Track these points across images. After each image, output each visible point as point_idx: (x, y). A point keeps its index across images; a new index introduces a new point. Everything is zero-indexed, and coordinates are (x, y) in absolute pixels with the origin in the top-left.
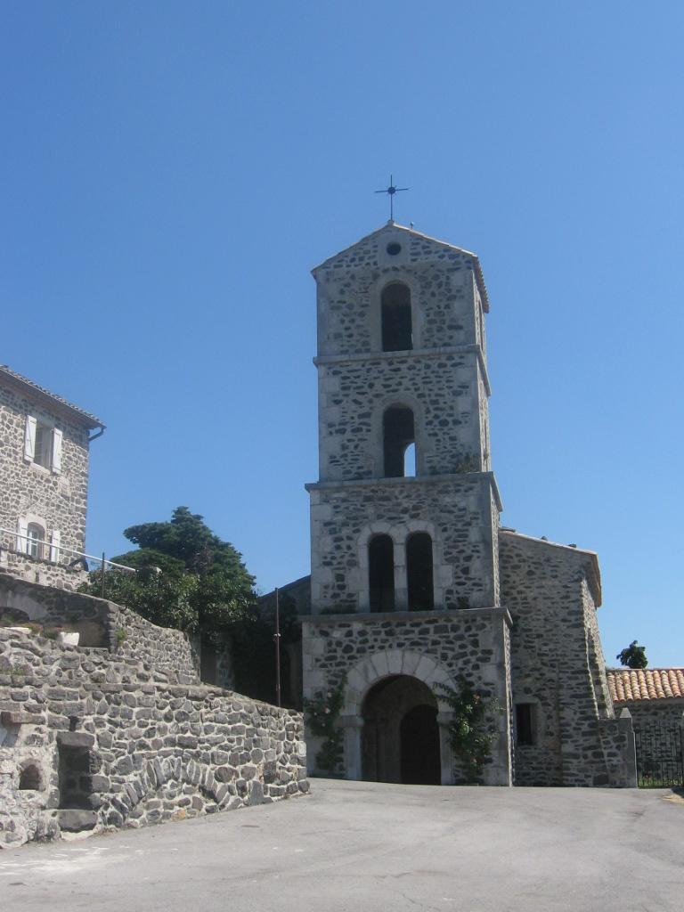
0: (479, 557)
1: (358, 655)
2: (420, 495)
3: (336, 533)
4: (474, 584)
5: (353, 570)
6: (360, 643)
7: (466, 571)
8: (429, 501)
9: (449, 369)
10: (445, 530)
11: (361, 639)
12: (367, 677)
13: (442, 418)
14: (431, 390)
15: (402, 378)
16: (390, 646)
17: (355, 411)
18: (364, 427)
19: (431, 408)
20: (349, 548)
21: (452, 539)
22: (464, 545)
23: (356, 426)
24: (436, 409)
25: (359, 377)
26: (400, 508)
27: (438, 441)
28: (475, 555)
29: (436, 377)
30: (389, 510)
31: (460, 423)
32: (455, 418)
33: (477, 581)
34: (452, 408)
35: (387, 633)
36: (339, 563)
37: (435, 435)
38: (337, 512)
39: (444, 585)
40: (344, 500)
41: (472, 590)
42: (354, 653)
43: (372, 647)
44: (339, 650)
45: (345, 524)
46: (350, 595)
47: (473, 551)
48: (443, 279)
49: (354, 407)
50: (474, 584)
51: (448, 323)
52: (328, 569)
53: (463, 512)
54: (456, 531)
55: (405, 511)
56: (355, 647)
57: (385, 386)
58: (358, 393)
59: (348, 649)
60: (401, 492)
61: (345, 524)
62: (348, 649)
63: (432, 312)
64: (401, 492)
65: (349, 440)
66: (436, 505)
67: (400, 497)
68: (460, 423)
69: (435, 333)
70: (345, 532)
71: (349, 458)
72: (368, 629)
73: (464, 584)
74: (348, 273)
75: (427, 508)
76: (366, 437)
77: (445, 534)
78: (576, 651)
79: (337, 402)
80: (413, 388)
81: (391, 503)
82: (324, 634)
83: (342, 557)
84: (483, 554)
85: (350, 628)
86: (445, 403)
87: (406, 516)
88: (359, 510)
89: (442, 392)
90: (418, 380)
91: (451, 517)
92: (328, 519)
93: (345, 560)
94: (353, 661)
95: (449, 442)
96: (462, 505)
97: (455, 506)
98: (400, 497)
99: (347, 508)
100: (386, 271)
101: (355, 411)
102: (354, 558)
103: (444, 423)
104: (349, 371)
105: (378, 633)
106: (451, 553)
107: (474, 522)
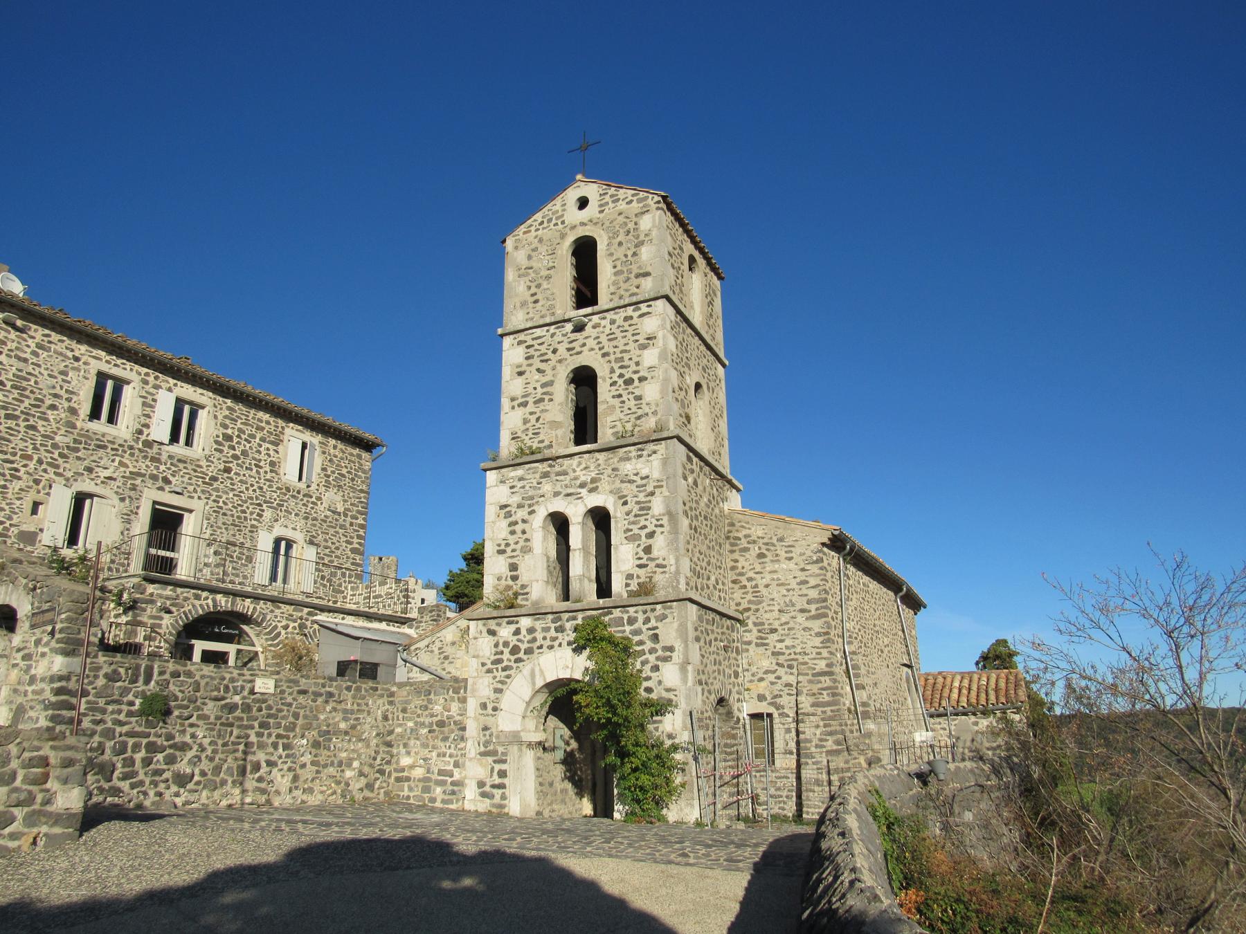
0: (662, 533)
1: (525, 657)
2: (599, 465)
3: (511, 516)
4: (658, 566)
5: (526, 557)
6: (528, 642)
7: (648, 550)
8: (610, 471)
9: (635, 320)
10: (625, 503)
11: (529, 637)
12: (534, 684)
13: (627, 376)
14: (616, 347)
15: (586, 338)
16: (560, 645)
17: (537, 381)
18: (547, 398)
19: (616, 366)
20: (524, 532)
21: (633, 514)
22: (646, 520)
23: (539, 396)
24: (621, 367)
25: (542, 344)
26: (578, 482)
27: (623, 402)
28: (659, 530)
29: (622, 331)
30: (566, 486)
31: (646, 379)
32: (641, 374)
33: (660, 561)
34: (637, 364)
35: (557, 630)
36: (513, 551)
37: (620, 396)
38: (513, 493)
39: (623, 569)
40: (521, 479)
41: (655, 572)
42: (521, 655)
43: (541, 647)
44: (506, 651)
45: (520, 506)
46: (523, 587)
47: (656, 526)
48: (631, 226)
49: (537, 376)
50: (658, 566)
51: (635, 271)
52: (501, 558)
53: (644, 482)
54: (638, 503)
55: (582, 485)
56: (523, 647)
57: (569, 350)
58: (542, 361)
59: (515, 650)
60: (580, 464)
61: (520, 506)
62: (515, 650)
63: (618, 263)
64: (580, 464)
65: (531, 413)
66: (616, 475)
67: (578, 469)
68: (646, 379)
69: (622, 284)
70: (521, 514)
71: (530, 433)
72: (539, 625)
73: (647, 565)
74: (536, 237)
75: (607, 479)
76: (547, 408)
77: (626, 508)
78: (818, 648)
79: (520, 374)
80: (597, 347)
81: (568, 478)
82: (492, 633)
83: (517, 543)
84: (666, 529)
85: (517, 626)
86: (630, 359)
87: (584, 491)
88: (535, 488)
89: (627, 348)
90: (604, 339)
91: (633, 487)
92: (503, 502)
93: (518, 547)
94: (520, 665)
95: (633, 402)
96: (644, 472)
97: (636, 474)
98: (578, 469)
99: (523, 487)
100: (573, 228)
101: (537, 381)
102: (528, 544)
103: (629, 382)
104: (533, 339)
105: (547, 629)
106: (631, 530)
107: (658, 491)
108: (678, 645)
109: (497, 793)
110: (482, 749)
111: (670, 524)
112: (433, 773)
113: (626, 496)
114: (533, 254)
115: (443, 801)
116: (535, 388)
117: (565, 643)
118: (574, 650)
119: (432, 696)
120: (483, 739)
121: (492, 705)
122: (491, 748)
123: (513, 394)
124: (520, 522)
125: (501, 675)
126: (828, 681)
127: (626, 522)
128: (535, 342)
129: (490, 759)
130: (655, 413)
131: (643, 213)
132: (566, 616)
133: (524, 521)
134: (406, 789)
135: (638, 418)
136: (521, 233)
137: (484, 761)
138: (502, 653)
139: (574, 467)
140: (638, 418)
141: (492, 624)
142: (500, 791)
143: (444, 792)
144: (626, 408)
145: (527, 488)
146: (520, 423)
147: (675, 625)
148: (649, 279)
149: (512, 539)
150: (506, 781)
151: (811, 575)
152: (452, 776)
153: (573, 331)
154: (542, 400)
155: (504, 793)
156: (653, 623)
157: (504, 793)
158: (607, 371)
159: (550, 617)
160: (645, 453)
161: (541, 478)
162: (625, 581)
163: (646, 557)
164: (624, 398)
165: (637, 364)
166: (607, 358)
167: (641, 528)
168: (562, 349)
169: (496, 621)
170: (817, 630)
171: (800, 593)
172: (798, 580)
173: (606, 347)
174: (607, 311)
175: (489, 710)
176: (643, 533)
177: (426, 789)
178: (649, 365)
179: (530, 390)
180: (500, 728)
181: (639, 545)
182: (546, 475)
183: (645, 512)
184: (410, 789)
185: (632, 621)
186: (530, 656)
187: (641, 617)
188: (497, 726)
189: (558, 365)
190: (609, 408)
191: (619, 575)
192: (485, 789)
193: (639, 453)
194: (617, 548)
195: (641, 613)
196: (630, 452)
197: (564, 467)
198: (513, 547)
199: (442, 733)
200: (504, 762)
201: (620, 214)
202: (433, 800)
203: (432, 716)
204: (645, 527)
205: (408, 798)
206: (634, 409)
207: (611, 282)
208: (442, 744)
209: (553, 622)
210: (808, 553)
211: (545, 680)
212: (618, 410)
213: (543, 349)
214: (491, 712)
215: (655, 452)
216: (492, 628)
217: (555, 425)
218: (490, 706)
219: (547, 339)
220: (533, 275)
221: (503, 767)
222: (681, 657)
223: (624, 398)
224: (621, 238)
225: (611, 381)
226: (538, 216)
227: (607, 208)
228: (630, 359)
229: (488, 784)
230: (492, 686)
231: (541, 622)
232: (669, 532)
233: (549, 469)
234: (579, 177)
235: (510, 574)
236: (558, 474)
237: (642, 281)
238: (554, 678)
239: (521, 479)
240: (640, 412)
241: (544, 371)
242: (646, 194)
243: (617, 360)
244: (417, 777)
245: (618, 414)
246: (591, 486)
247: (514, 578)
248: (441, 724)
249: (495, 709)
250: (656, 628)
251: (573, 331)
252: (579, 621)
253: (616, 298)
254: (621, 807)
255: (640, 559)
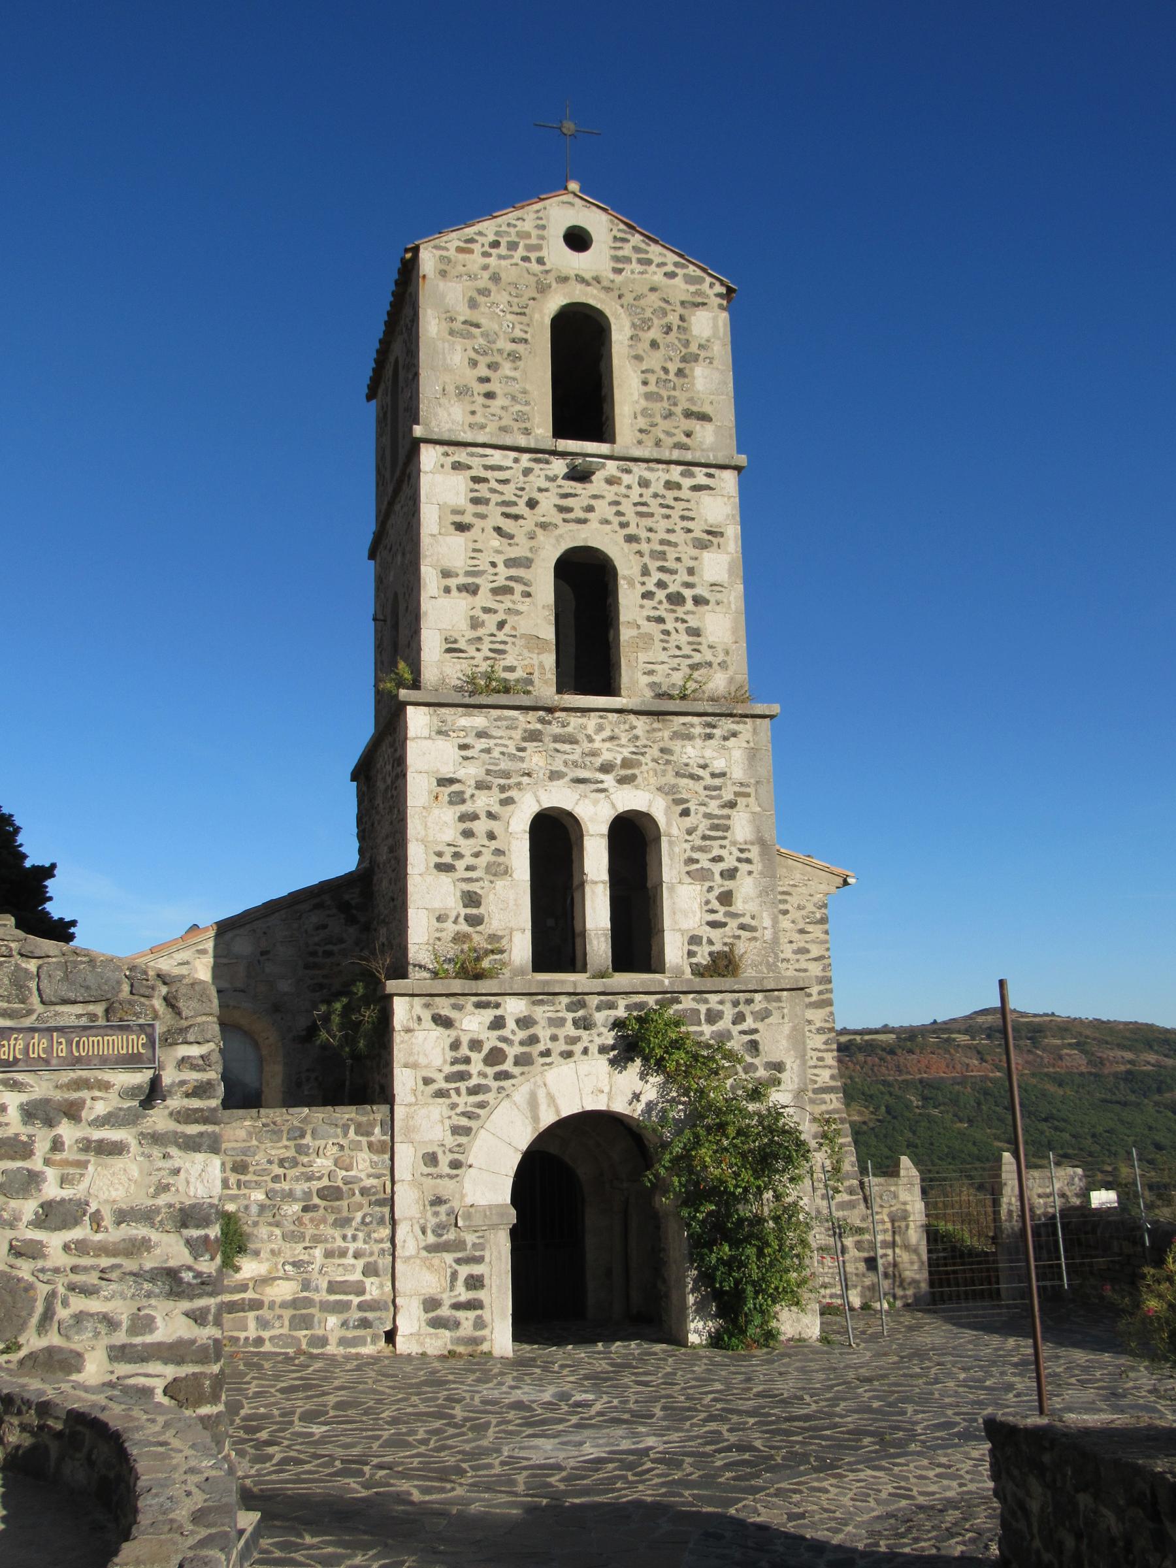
0: (750, 873)
1: (516, 1071)
2: (637, 738)
3: (463, 801)
4: (742, 927)
5: (499, 884)
6: (522, 1043)
7: (726, 898)
8: (654, 752)
9: (685, 493)
10: (685, 813)
11: (522, 1035)
12: (536, 1119)
13: (672, 588)
14: (650, 530)
15: (595, 497)
16: (585, 1051)
17: (498, 552)
18: (519, 588)
19: (653, 565)
20: (491, 836)
21: (699, 833)
22: (722, 847)
23: (501, 581)
24: (661, 569)
25: (505, 482)
26: (598, 761)
27: (667, 633)
28: (744, 867)
29: (662, 506)
30: (575, 764)
31: (707, 602)
32: (698, 591)
33: (746, 920)
34: (691, 571)
35: (576, 1023)
36: (469, 868)
37: (660, 620)
38: (466, 758)
39: (685, 926)
40: (481, 734)
41: (739, 937)
42: (508, 1066)
43: (547, 1053)
44: (477, 1058)
45: (481, 786)
46: (493, 938)
47: (739, 860)
48: (673, 319)
49: (496, 542)
50: (742, 927)
51: (683, 404)
52: (445, 879)
53: (717, 782)
54: (708, 816)
55: (606, 768)
56: (512, 1051)
57: (562, 509)
58: (506, 515)
59: (495, 1057)
60: (600, 728)
61: (481, 786)
62: (495, 1057)
63: (652, 379)
64: (600, 728)
65: (487, 610)
66: (668, 762)
67: (598, 738)
68: (707, 602)
69: (658, 419)
70: (483, 802)
71: (485, 647)
72: (541, 1013)
73: (724, 925)
74: (485, 267)
75: (652, 765)
76: (520, 607)
77: (688, 822)
78: (820, 1051)
79: (461, 527)
80: (616, 520)
81: (578, 749)
82: (444, 1022)
83: (477, 855)
84: (757, 867)
85: (498, 1012)
86: (678, 559)
87: (609, 780)
88: (512, 757)
89: (672, 538)
90: (627, 507)
91: (698, 787)
92: (447, 772)
93: (482, 862)
94: (506, 1084)
95: (684, 638)
96: (719, 765)
97: (704, 767)
98: (598, 738)
99: (488, 751)
100: (564, 280)
101: (498, 552)
102: (501, 859)
103: (676, 599)
104: (486, 467)
105: (560, 1022)
106: (697, 861)
107: (741, 801)
108: (792, 1063)
109: (467, 1318)
110: (431, 1239)
111: (762, 860)
112: (317, 1290)
113: (687, 801)
114: (481, 299)
115: (343, 1342)
116: (494, 565)
117: (594, 1049)
118: (613, 1062)
119: (308, 1140)
120: (433, 1221)
121: (450, 1157)
122: (451, 1235)
123: (448, 564)
124: (483, 816)
125: (465, 1101)
126: (834, 1100)
127: (687, 846)
128: (489, 474)
129: (449, 1258)
130: (723, 665)
131: (697, 305)
132: (594, 1001)
133: (491, 815)
134: (252, 1325)
135: (694, 667)
136: (452, 246)
137: (436, 1262)
138: (467, 1061)
139: (590, 730)
140: (694, 667)
141: (444, 1007)
142: (472, 1315)
143: (344, 1324)
144: (671, 645)
145: (496, 753)
146: (464, 625)
147: (787, 1029)
148: (709, 427)
149: (466, 847)
150: (481, 1295)
151: (813, 941)
152: (361, 1291)
153: (568, 477)
154: (505, 590)
155: (479, 1317)
156: (749, 1023)
157: (479, 1317)
158: (636, 571)
159: (565, 1000)
160: (717, 732)
161: (524, 739)
162: (686, 948)
163: (722, 910)
164: (669, 626)
165: (691, 571)
166: (635, 546)
167: (713, 860)
168: (547, 503)
169: (452, 1000)
170: (818, 1025)
171: (797, 966)
172: (795, 946)
173: (633, 525)
174: (635, 460)
175: (444, 1168)
176: (717, 868)
177: (305, 1322)
178: (712, 580)
179: (484, 565)
180: (469, 1200)
181: (710, 889)
182: (533, 736)
183: (720, 834)
184: (263, 1324)
185: (713, 1017)
186: (526, 1069)
187: (729, 1012)
188: (463, 1196)
189: (539, 531)
190: (640, 636)
191: (678, 935)
192: (439, 1312)
193: (708, 731)
194: (672, 889)
195: (728, 1005)
196: (692, 726)
197: (569, 729)
198: (469, 860)
199: (334, 1210)
200: (479, 1260)
201: (653, 289)
202: (323, 1341)
203: (309, 1178)
204: (718, 859)
205: (259, 1341)
206: (687, 650)
207: (638, 408)
208: (337, 1233)
209: (570, 1008)
210: (810, 907)
211: (558, 1112)
212: (658, 645)
213: (509, 492)
214: (447, 1170)
215: (734, 735)
216: (443, 1012)
217: (534, 641)
218: (444, 1160)
219: (515, 474)
220: (481, 341)
221: (477, 1270)
222: (796, 1080)
223: (669, 626)
224: (654, 333)
225: (643, 589)
226: (488, 228)
227: (628, 267)
228: (678, 559)
229: (447, 1303)
230: (447, 1123)
231: (546, 1008)
232: (761, 873)
233: (539, 726)
234: (573, 186)
235: (464, 912)
236: (557, 739)
237: (696, 426)
238: (576, 1109)
239: (481, 734)
240: (697, 658)
241: (511, 537)
242: (699, 273)
243: (655, 555)
244: (278, 1300)
245: (656, 653)
246: (623, 772)
247: (474, 921)
248: (331, 1194)
249: (456, 1165)
250: (755, 1031)
251: (568, 477)
252: (621, 1013)
253: (649, 441)
254: (700, 1325)
255: (713, 911)
